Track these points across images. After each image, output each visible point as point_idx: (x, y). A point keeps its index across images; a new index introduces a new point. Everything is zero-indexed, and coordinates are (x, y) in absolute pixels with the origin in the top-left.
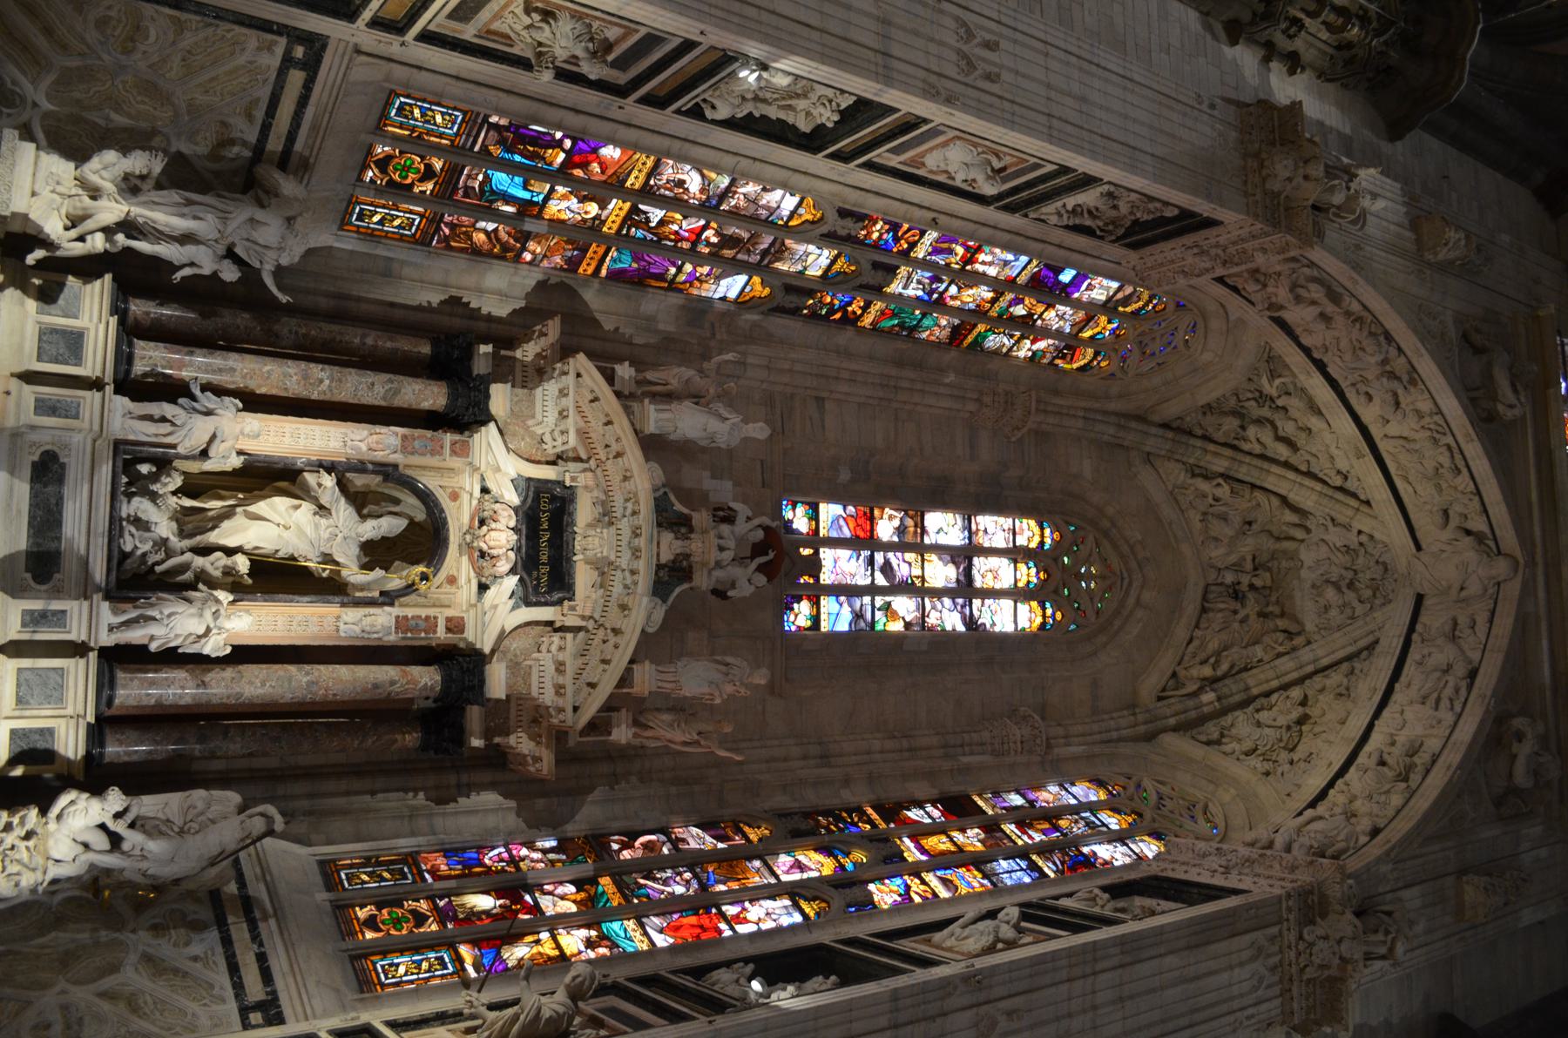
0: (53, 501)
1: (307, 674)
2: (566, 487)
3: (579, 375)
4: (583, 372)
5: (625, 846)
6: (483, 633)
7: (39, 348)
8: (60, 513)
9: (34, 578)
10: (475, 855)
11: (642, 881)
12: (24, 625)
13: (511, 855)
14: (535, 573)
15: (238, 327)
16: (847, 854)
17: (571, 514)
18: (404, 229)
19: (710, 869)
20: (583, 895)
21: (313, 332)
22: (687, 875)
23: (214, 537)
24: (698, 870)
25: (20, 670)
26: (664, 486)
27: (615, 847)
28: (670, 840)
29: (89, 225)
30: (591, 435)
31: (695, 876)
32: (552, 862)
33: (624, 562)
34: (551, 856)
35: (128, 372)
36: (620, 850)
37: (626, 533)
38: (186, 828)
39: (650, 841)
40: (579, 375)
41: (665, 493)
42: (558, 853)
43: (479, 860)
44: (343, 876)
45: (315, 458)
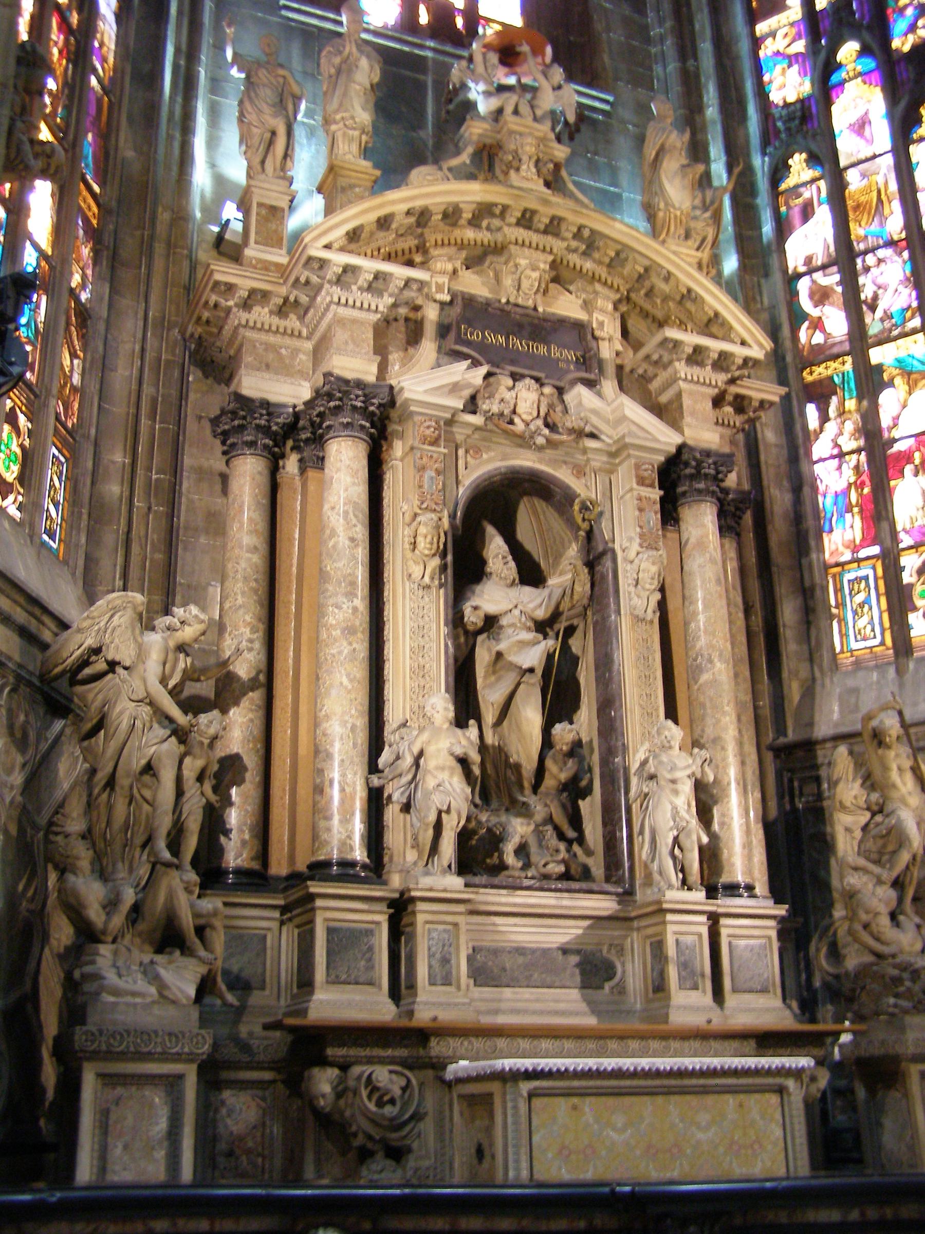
0: (521, 960)
1: (710, 661)
2: (451, 302)
3: (328, 247)
4: (325, 241)
5: (818, 324)
6: (656, 440)
7: (357, 983)
8: (533, 951)
9: (611, 978)
10: (829, 500)
11: (879, 313)
12: (695, 987)
13: (833, 457)
14: (561, 365)
15: (251, 720)
16: (840, 66)
17: (488, 303)
18: (61, 472)
19: (861, 232)
20: (898, 381)
21: (248, 618)
22: (870, 259)
23: (529, 766)
24: (862, 246)
25: (735, 990)
26: (441, 169)
27: (818, 338)
28: (809, 272)
29: (187, 921)
30: (399, 249)
31: (873, 250)
32: (842, 413)
33: (558, 245)
34: (832, 411)
35: (364, 867)
36: (823, 330)
37: (522, 233)
38: (875, 808)
39: (811, 296)
40: (328, 247)
41: (450, 169)
42: (828, 405)
43: (836, 495)
44: (862, 644)
45: (444, 630)
